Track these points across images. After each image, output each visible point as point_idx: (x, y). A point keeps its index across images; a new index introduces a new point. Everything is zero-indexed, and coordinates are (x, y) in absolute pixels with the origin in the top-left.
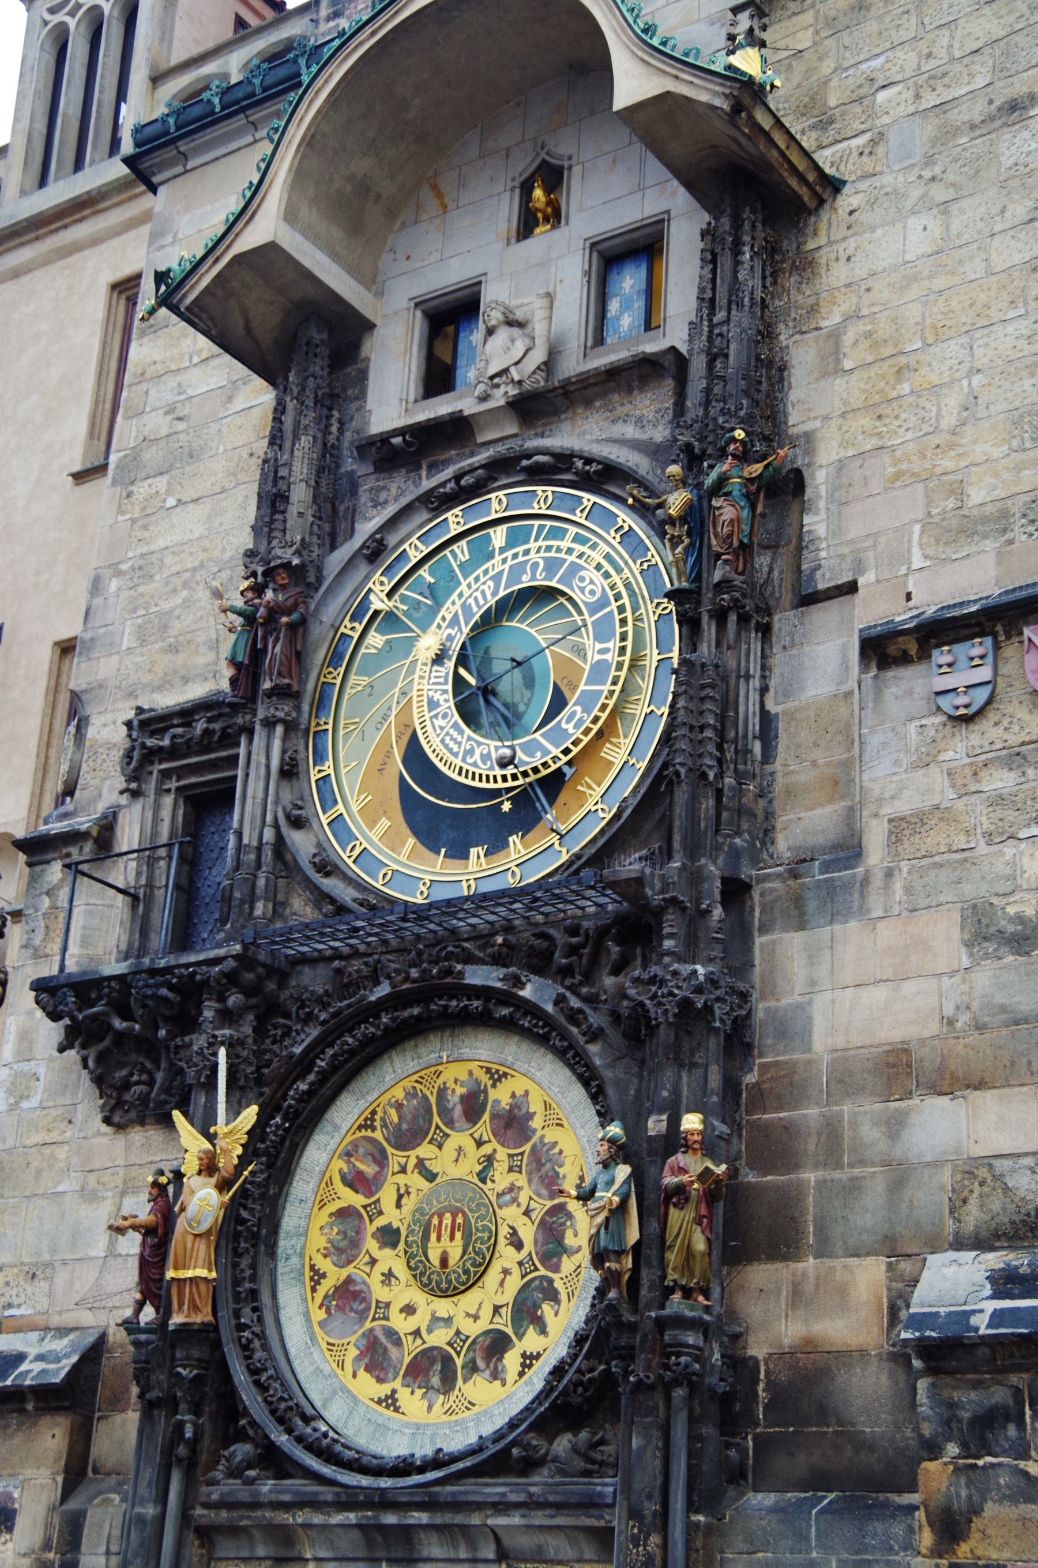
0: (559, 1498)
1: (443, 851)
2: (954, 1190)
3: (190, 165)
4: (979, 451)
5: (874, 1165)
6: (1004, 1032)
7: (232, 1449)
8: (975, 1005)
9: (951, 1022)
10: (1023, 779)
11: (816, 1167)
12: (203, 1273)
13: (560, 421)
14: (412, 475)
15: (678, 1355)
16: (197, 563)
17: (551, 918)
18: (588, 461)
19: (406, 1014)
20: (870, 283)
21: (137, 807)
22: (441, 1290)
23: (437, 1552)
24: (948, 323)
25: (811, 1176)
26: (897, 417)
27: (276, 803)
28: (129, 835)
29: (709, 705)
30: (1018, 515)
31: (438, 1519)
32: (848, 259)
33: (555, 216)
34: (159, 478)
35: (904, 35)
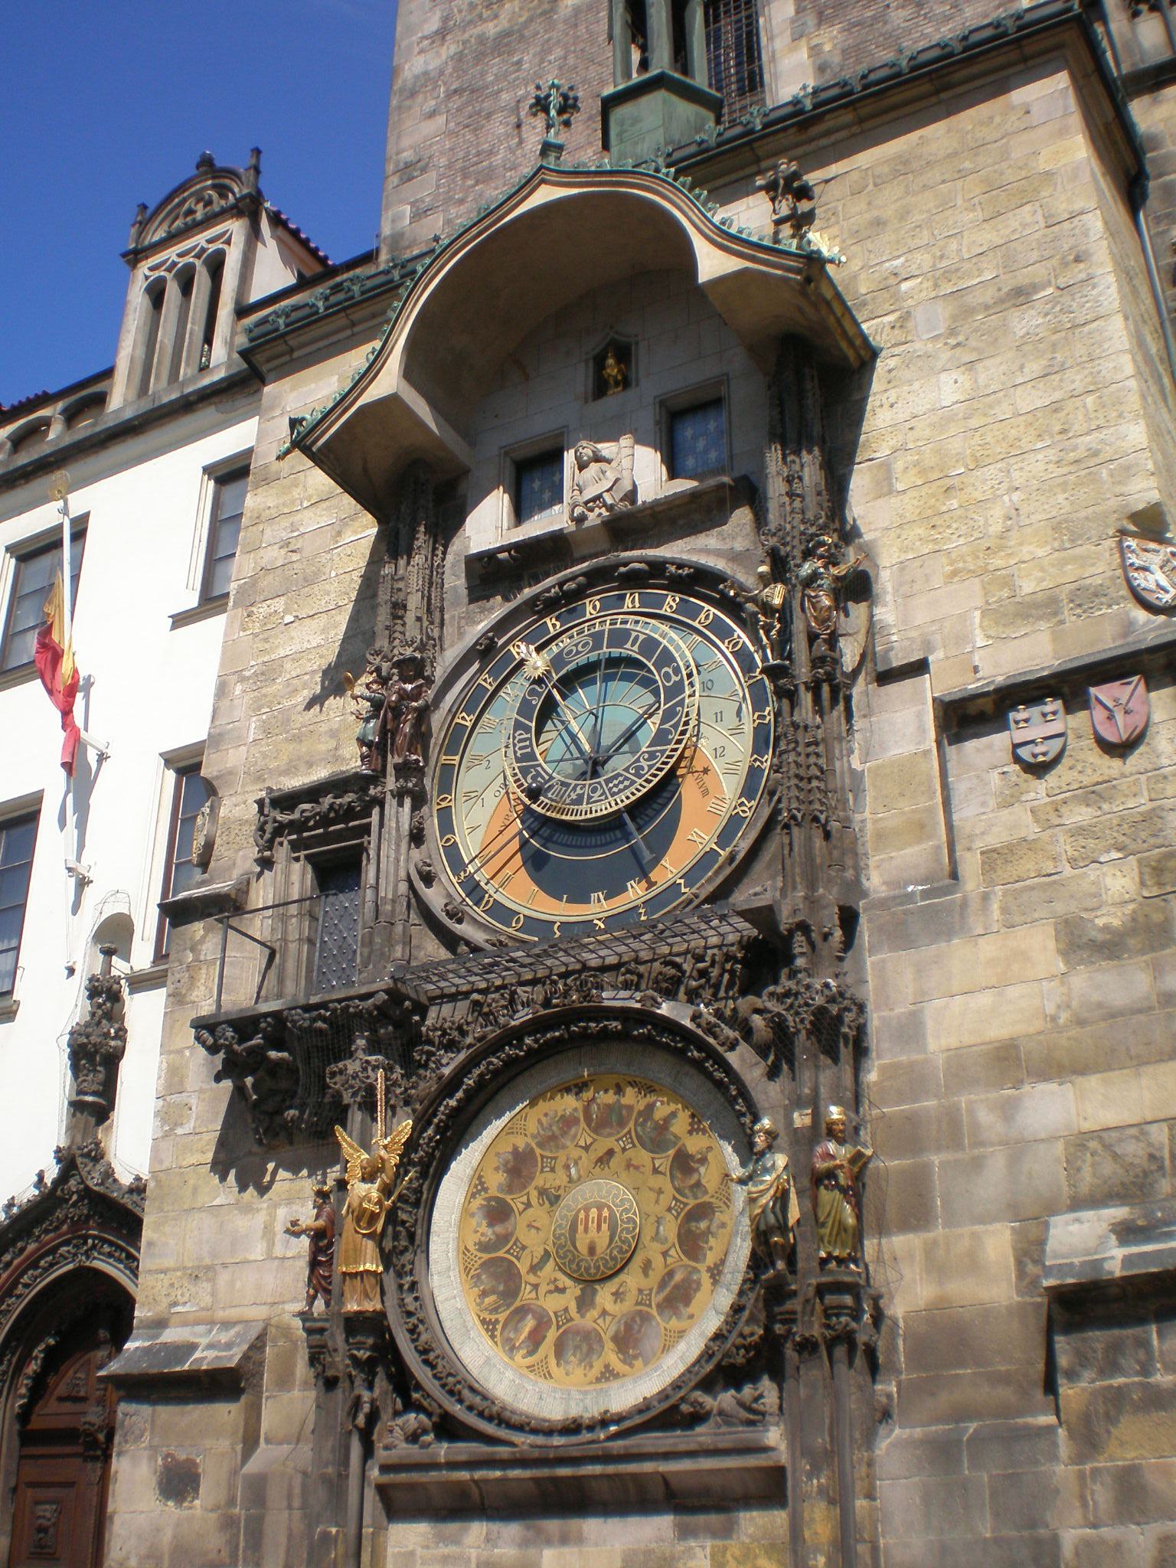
2: (1067, 1161)
3: (296, 355)
4: (1025, 552)
5: (992, 1144)
6: (1103, 1024)
8: (1074, 1004)
10: (1099, 813)
11: (939, 1149)
12: (373, 1268)
15: (838, 1315)
17: (675, 949)
18: (680, 566)
20: (913, 423)
24: (986, 453)
25: (936, 1159)
26: (949, 527)
27: (407, 860)
28: (262, 894)
29: (812, 760)
31: (611, 1469)
33: (625, 383)
35: (918, 242)
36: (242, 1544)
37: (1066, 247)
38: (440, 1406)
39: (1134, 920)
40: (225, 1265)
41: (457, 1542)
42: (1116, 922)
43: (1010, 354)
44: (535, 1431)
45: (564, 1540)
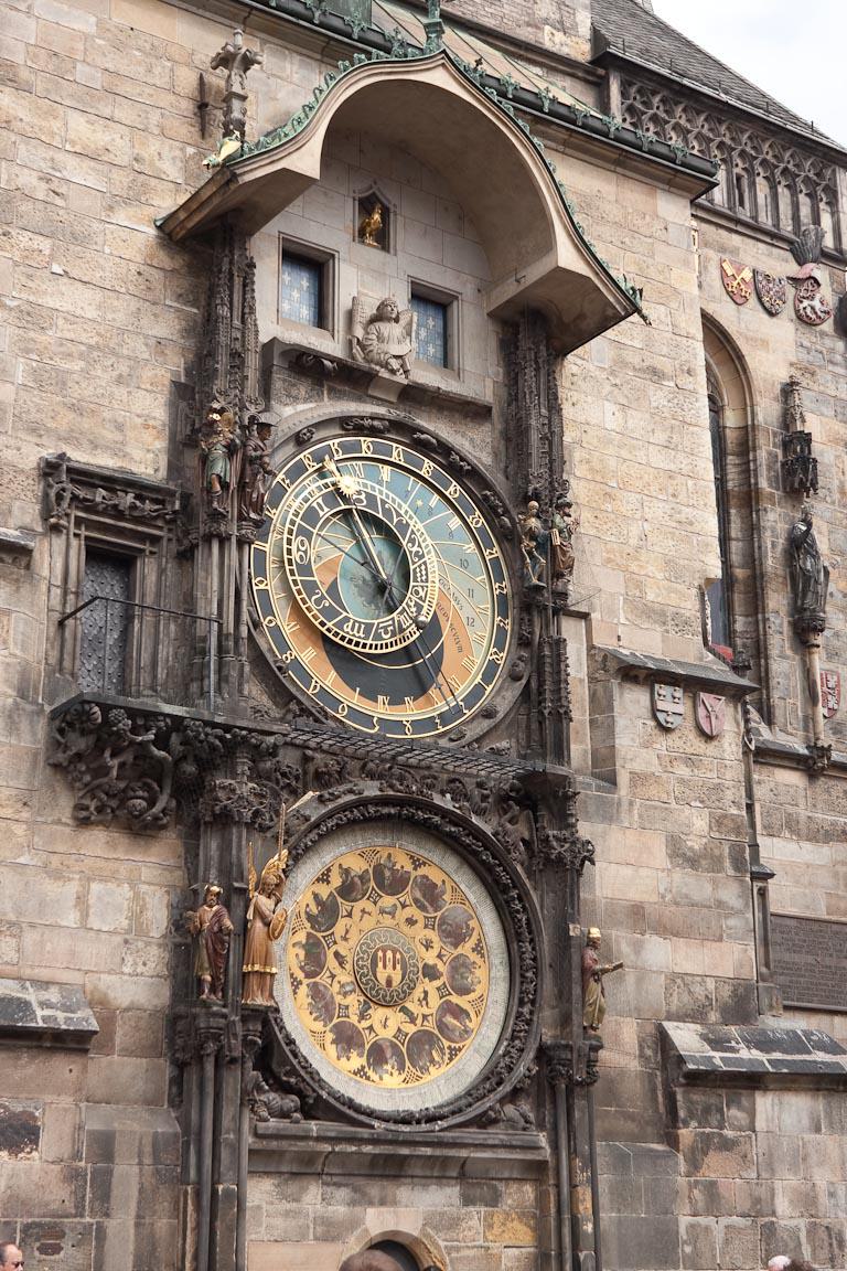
0: (519, 1143)
1: (358, 689)
4: (651, 569)
6: (687, 908)
7: (272, 1095)
8: (674, 890)
9: (663, 897)
13: (420, 409)
14: (317, 387)
16: (93, 342)
18: (462, 459)
19: (385, 810)
20: (586, 428)
21: (58, 542)
22: (385, 1001)
23: (418, 1172)
30: (669, 618)
31: (438, 1152)
32: (573, 404)
34: (41, 238)
36: (88, 1196)
37: (683, 358)
38: (314, 1091)
39: (705, 849)
40: (32, 926)
41: (297, 1200)
42: (696, 847)
43: (647, 416)
44: (378, 1118)
45: (383, 1203)
